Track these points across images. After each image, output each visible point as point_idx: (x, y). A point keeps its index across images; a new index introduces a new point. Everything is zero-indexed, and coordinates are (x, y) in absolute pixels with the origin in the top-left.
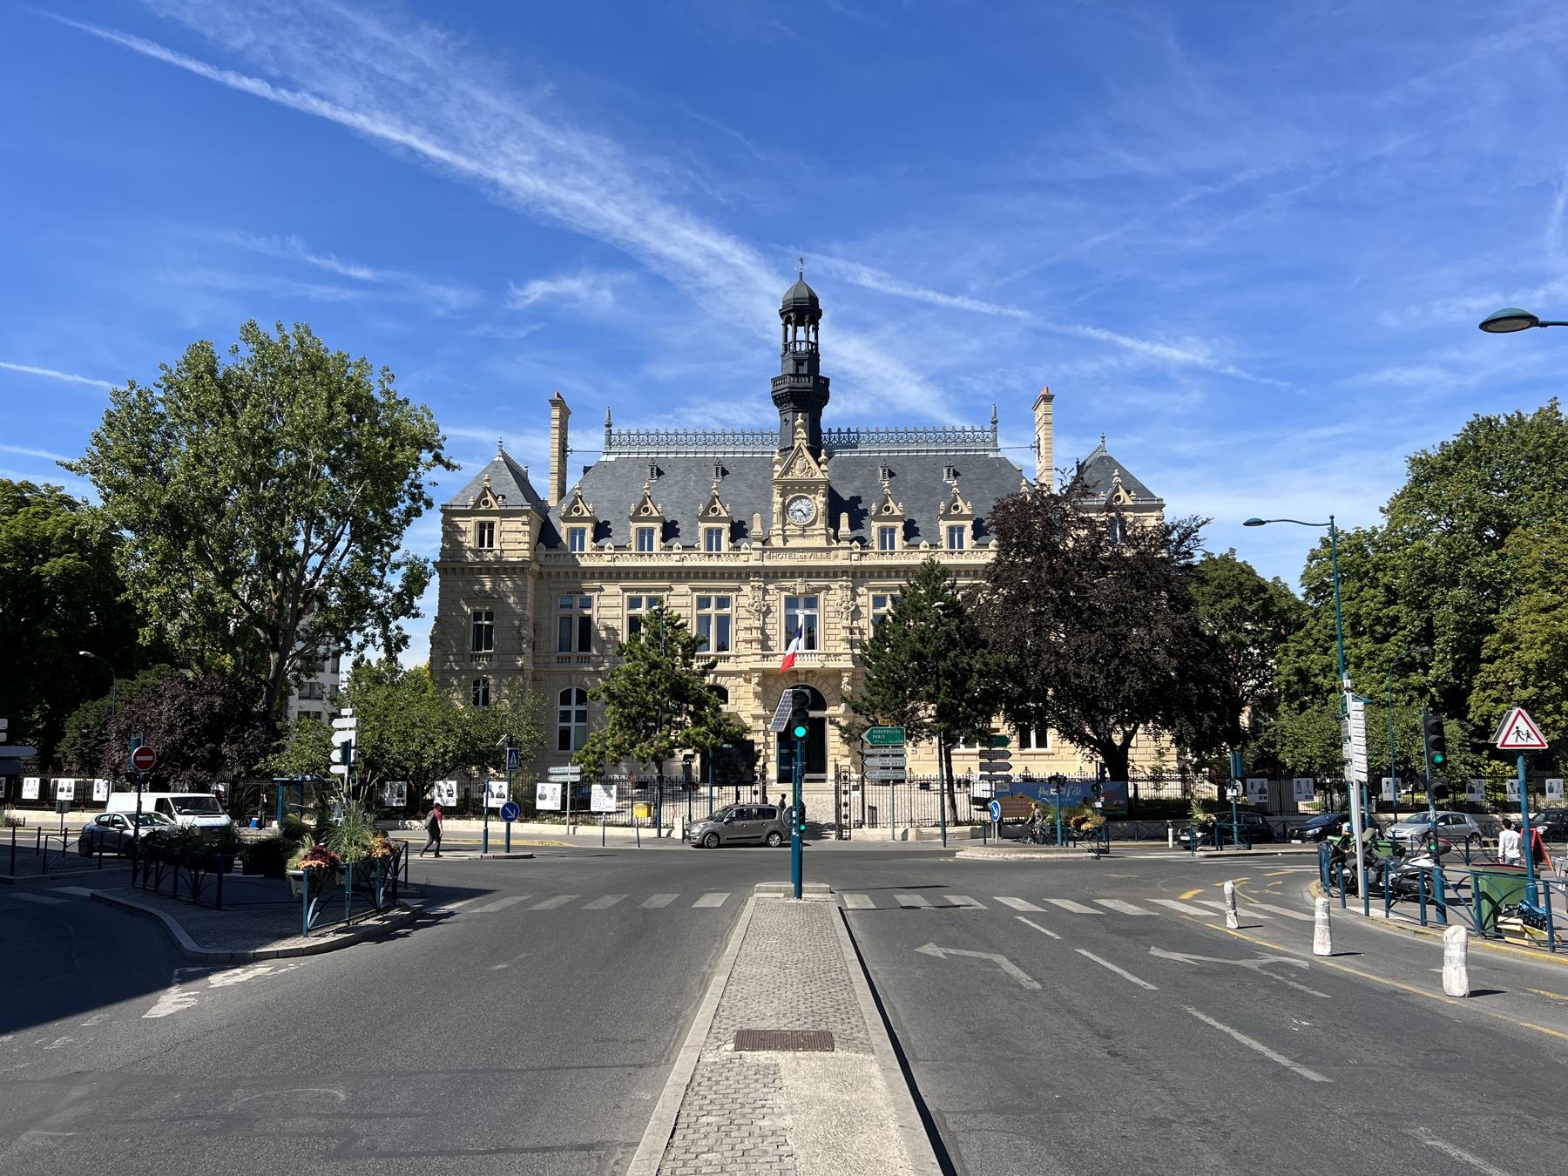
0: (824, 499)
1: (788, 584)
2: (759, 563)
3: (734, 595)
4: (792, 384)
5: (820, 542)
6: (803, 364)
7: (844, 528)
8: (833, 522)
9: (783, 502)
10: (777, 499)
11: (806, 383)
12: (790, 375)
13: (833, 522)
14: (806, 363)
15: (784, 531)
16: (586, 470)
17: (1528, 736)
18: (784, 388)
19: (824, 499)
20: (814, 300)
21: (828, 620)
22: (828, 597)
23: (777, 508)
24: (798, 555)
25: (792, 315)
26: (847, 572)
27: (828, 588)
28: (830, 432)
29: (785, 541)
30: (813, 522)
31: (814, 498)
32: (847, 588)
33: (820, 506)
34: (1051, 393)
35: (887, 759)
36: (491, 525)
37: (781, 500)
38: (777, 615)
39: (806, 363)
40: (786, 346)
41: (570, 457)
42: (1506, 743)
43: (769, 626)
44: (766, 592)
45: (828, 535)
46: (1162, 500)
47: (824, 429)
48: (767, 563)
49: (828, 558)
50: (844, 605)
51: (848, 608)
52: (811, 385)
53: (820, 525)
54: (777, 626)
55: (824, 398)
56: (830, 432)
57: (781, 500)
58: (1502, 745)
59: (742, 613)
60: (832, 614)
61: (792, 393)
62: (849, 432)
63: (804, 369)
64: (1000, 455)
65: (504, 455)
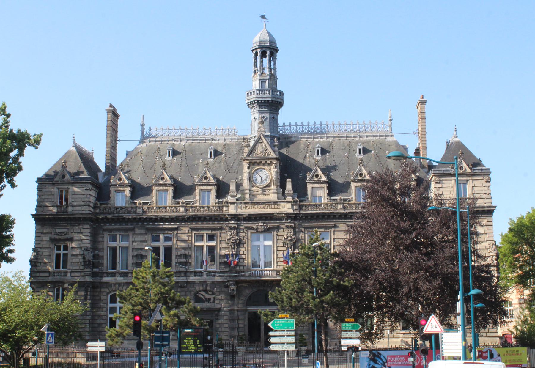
0: (275, 170)
1: (253, 226)
2: (234, 212)
3: (218, 232)
4: (258, 96)
5: (273, 196)
6: (265, 82)
7: (289, 185)
8: (283, 186)
9: (250, 173)
10: (246, 170)
11: (268, 95)
12: (257, 90)
13: (283, 186)
14: (267, 82)
15: (250, 190)
16: (128, 153)
17: (436, 327)
18: (253, 97)
19: (275, 170)
20: (272, 42)
21: (279, 249)
22: (279, 234)
23: (246, 176)
24: (259, 206)
25: (258, 51)
26: (291, 217)
27: (278, 228)
28: (284, 125)
29: (252, 195)
30: (268, 186)
31: (270, 170)
32: (291, 227)
33: (274, 175)
34: (424, 99)
35: (283, 338)
36: (67, 191)
37: (248, 171)
38: (246, 245)
39: (267, 82)
40: (255, 70)
41: (119, 145)
42: (440, 330)
43: (241, 253)
44: (238, 229)
45: (278, 193)
46: (489, 169)
47: (280, 123)
48: (240, 211)
49: (278, 208)
50: (289, 238)
51: (291, 240)
52: (270, 95)
53: (273, 187)
54: (246, 253)
55: (281, 104)
56: (284, 125)
57: (248, 171)
58: (425, 331)
59: (224, 245)
60: (281, 245)
61: (258, 101)
62: (296, 125)
63: (266, 85)
64: (394, 139)
65: (76, 146)
